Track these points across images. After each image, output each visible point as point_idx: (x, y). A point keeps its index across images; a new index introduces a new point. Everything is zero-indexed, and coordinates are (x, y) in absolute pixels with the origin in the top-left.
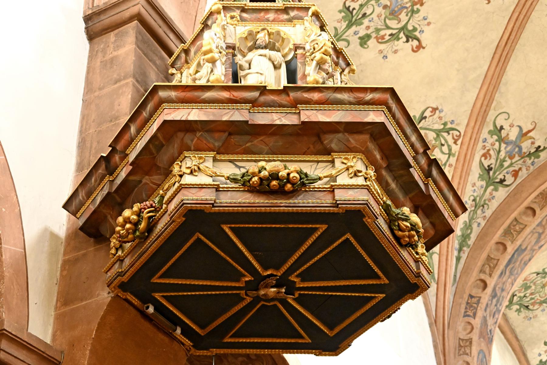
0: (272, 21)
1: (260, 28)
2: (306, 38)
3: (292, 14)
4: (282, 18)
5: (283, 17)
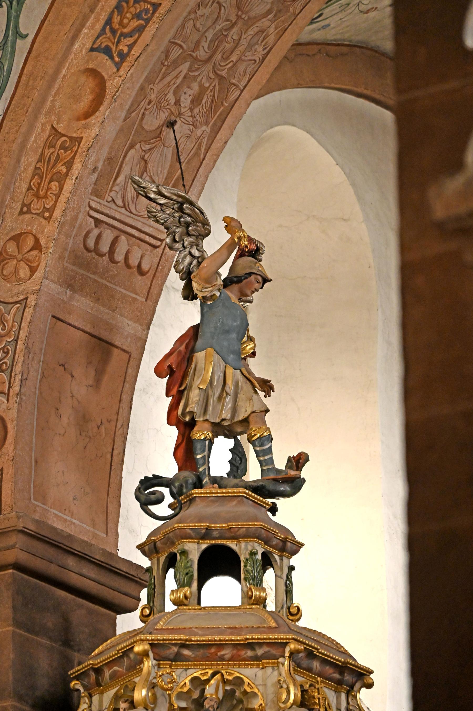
0: (229, 660)
1: (210, 672)
2: (282, 705)
3: (260, 652)
4: (245, 656)
5: (246, 653)
